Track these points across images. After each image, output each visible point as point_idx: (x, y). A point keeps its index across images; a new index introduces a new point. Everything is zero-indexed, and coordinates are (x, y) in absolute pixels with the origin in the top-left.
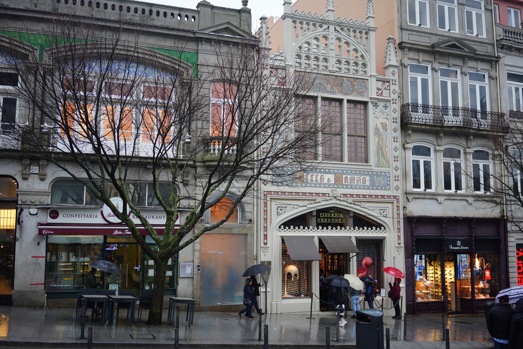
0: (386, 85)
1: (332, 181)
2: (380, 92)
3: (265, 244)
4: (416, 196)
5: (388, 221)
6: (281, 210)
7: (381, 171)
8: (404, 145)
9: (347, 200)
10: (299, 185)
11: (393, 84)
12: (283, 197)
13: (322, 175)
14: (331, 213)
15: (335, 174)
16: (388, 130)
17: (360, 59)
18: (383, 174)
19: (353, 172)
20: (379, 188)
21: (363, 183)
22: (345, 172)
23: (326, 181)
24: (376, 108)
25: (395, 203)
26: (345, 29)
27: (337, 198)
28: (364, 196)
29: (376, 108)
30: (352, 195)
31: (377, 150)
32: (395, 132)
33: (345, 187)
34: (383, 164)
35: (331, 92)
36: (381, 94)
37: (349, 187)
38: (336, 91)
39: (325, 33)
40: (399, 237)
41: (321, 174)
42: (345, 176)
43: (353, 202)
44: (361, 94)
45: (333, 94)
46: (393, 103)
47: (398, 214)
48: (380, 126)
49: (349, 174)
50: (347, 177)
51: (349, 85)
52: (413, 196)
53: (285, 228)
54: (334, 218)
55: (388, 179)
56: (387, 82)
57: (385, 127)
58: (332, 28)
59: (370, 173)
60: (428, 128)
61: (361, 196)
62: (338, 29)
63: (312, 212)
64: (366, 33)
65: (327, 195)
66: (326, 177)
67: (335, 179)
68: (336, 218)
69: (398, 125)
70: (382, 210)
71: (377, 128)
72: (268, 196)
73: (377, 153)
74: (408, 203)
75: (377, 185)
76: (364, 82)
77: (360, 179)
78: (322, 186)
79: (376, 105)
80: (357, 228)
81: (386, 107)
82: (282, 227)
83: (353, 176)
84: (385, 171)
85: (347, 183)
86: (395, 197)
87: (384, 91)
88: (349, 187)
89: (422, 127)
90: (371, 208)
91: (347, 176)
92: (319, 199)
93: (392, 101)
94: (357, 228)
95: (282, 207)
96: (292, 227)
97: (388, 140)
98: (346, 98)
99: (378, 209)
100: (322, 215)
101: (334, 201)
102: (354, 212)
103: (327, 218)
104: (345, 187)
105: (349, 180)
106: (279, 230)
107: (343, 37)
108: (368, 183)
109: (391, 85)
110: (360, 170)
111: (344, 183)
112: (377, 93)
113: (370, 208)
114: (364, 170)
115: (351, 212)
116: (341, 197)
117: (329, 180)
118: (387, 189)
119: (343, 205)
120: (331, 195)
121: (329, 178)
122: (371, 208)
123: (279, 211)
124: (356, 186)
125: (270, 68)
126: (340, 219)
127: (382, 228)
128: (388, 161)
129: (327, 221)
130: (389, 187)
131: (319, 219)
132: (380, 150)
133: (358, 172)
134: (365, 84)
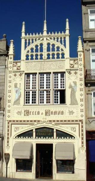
2: (72, 66)
3: (8, 145)
5: (76, 134)
11: (80, 61)
16: (77, 85)
17: (60, 50)
24: (70, 74)
26: (52, 38)
29: (70, 74)
36: (73, 67)
39: (41, 42)
40: (83, 143)
46: (80, 71)
47: (82, 131)
52: (92, 120)
53: (18, 138)
54: (46, 133)
56: (76, 60)
57: (75, 83)
58: (45, 39)
61: (78, 121)
62: (48, 38)
63: (32, 130)
64: (65, 38)
65: (40, 121)
67: (46, 113)
70: (73, 128)
72: (10, 122)
77: (60, 112)
79: (70, 73)
81: (76, 73)
82: (17, 137)
86: (80, 121)
87: (75, 65)
92: (36, 123)
93: (79, 70)
96: (22, 137)
98: (52, 71)
102: (57, 130)
109: (79, 62)
112: (70, 66)
113: (65, 127)
115: (54, 129)
119: (50, 126)
120: (42, 121)
123: (16, 129)
127: (73, 138)
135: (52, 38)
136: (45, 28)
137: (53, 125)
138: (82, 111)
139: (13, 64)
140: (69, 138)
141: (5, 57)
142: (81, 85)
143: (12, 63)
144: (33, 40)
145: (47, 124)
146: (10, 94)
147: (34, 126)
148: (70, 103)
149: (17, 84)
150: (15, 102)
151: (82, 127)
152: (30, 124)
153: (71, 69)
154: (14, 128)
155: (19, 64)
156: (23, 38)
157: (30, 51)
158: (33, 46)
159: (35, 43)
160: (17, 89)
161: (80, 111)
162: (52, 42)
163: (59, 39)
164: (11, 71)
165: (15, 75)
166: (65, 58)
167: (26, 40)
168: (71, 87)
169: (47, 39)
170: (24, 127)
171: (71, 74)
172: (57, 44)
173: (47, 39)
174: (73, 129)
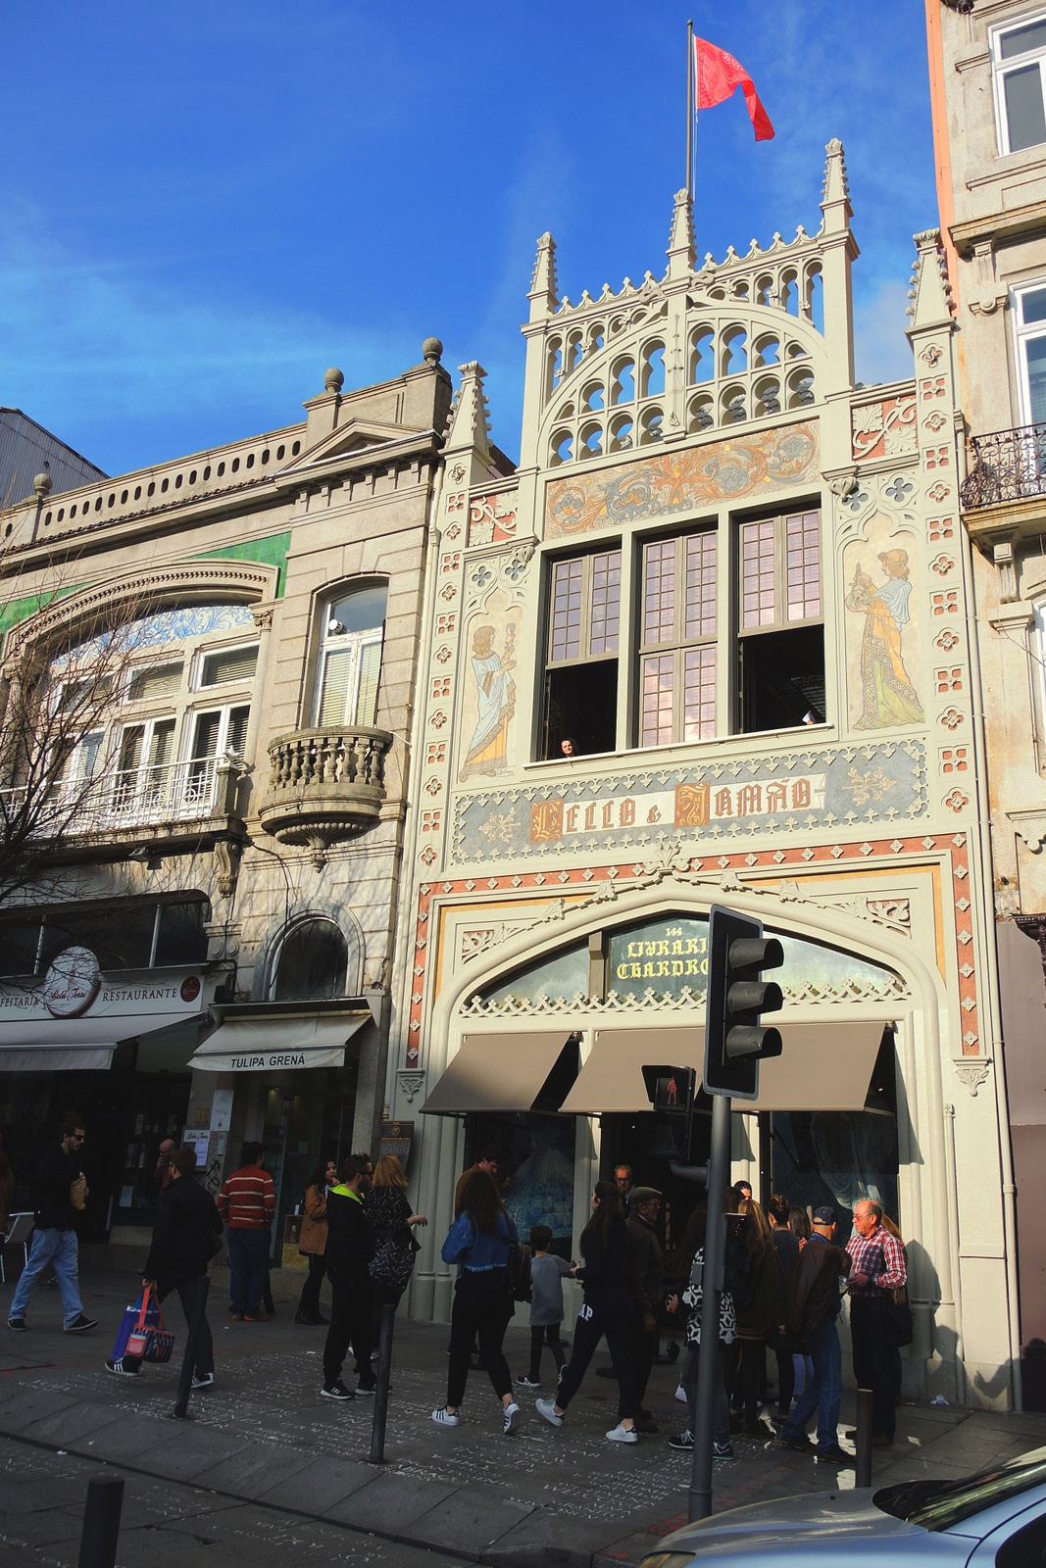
0: (899, 411)
1: (668, 817)
2: (871, 443)
7: (878, 742)
10: (543, 847)
12: (481, 895)
13: (628, 801)
14: (673, 939)
15: (678, 788)
23: (641, 820)
25: (946, 862)
28: (792, 854)
30: (736, 859)
33: (716, 829)
34: (891, 712)
35: (670, 509)
36: (879, 448)
37: (734, 828)
38: (692, 497)
39: (649, 332)
40: (967, 1019)
41: (625, 798)
43: (740, 885)
44: (791, 477)
45: (681, 510)
47: (962, 916)
48: (874, 570)
51: (743, 459)
57: (897, 566)
58: (677, 303)
64: (814, 268)
66: (643, 803)
67: (678, 807)
69: (956, 545)
71: (861, 581)
73: (863, 674)
75: (859, 801)
76: (805, 432)
77: (784, 788)
78: (627, 838)
81: (899, 491)
82: (477, 1000)
83: (753, 784)
85: (725, 816)
86: (941, 839)
90: (830, 901)
91: (729, 787)
92: (603, 888)
93: (924, 460)
95: (479, 933)
103: (655, 959)
105: (735, 802)
106: (465, 1013)
107: (717, 314)
108: (817, 801)
111: (713, 816)
113: (822, 902)
117: (653, 814)
118: (912, 809)
121: (655, 808)
122: (830, 901)
123: (470, 944)
124: (764, 820)
125: (472, 500)
128: (912, 697)
129: (656, 969)
130: (919, 802)
134: (811, 437)
135: (728, 287)
136: (680, 237)
139: (470, 510)
141: (426, 469)
142: (943, 567)
143: (465, 501)
144: (597, 331)
145: (686, 890)
146: (444, 704)
147: (594, 910)
148: (857, 712)
149: (491, 630)
150: (474, 752)
153: (853, 464)
154: (460, 936)
155: (505, 503)
156: (534, 333)
157: (579, 402)
158: (598, 366)
159: (609, 351)
160: (491, 664)
162: (719, 313)
163: (777, 286)
164: (456, 557)
165: (481, 577)
166: (819, 399)
167: (555, 343)
168: (862, 594)
169: (690, 303)
170: (528, 924)
171: (863, 505)
172: (758, 318)
173: (690, 303)
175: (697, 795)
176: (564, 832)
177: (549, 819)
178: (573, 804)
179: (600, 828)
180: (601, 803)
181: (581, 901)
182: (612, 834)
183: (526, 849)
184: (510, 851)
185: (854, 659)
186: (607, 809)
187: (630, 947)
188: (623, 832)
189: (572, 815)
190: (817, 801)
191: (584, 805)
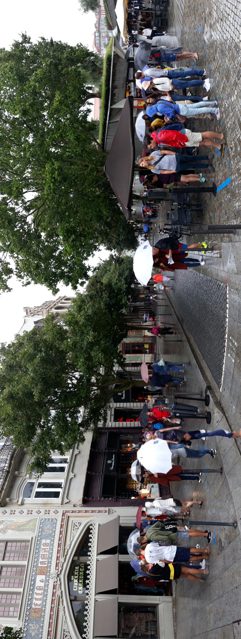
1: (43, 577)
4: (66, 495)
5: (84, 521)
6: (66, 636)
7: (39, 528)
8: (19, 505)
9: (62, 563)
10: (43, 614)
13: (36, 588)
15: (36, 574)
18: (41, 526)
19: (37, 555)
20: (54, 530)
21: (48, 546)
22: (35, 564)
23: (42, 584)
27: (59, 573)
28: (59, 545)
30: (58, 558)
31: (20, 531)
32: (6, 512)
37: (50, 560)
40: (99, 512)
41: (36, 589)
42: (39, 564)
43: (64, 557)
47: (79, 512)
49: (38, 560)
50: (40, 562)
54: (79, 576)
55: (47, 520)
59: (39, 539)
60: (6, 483)
66: (38, 584)
67: (41, 574)
68: (79, 573)
74: (70, 503)
75: (51, 532)
77: (43, 549)
80: (89, 553)
83: (40, 556)
84: (39, 523)
85: (47, 563)
86: (63, 514)
88: (50, 560)
89: (4, 488)
90: (72, 538)
92: (58, 593)
94: (89, 553)
95: (64, 634)
96: (85, 624)
97: (12, 520)
99: (73, 531)
100: (75, 588)
101: (62, 576)
102: (75, 555)
104: (49, 565)
108: (48, 541)
110: (35, 549)
111: (46, 566)
113: (72, 540)
114: (36, 545)
116: (58, 569)
119: (66, 567)
120: (56, 580)
121: (40, 580)
122: (72, 538)
124: (50, 553)
126: (81, 569)
127: (91, 527)
128: (30, 521)
130: (54, 520)
131: (79, 591)
132: (19, 528)
133: (37, 551)
137: (65, 560)
138: (47, 512)
140: (91, 533)
151: (73, 512)
152: (59, 605)
161: (47, 515)
170: (64, 617)
174: (76, 526)
175: (40, 570)
176: (40, 607)
177: (35, 612)
178: (33, 605)
179: (42, 596)
180: (35, 596)
181: (61, 600)
182: (44, 593)
183: (42, 619)
184: (42, 625)
185: (18, 533)
186: (37, 594)
187: (74, 590)
188: (44, 589)
189: (36, 605)
190: (48, 541)
191: (34, 601)
